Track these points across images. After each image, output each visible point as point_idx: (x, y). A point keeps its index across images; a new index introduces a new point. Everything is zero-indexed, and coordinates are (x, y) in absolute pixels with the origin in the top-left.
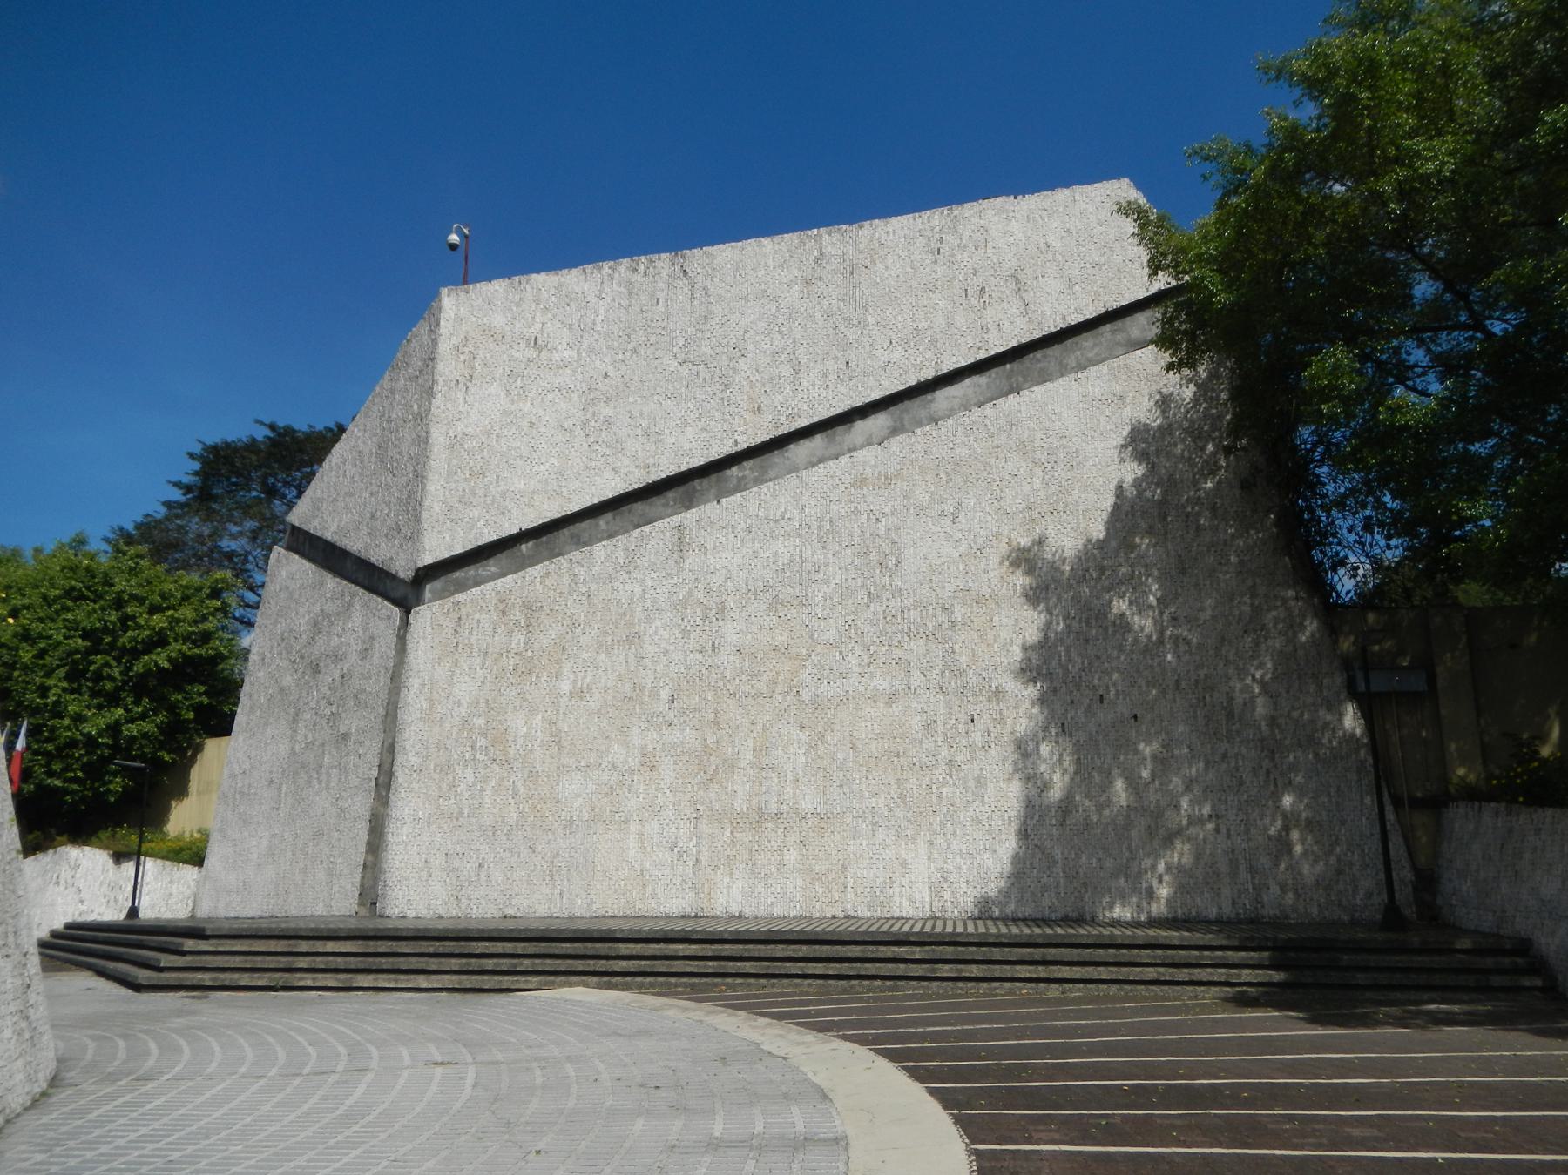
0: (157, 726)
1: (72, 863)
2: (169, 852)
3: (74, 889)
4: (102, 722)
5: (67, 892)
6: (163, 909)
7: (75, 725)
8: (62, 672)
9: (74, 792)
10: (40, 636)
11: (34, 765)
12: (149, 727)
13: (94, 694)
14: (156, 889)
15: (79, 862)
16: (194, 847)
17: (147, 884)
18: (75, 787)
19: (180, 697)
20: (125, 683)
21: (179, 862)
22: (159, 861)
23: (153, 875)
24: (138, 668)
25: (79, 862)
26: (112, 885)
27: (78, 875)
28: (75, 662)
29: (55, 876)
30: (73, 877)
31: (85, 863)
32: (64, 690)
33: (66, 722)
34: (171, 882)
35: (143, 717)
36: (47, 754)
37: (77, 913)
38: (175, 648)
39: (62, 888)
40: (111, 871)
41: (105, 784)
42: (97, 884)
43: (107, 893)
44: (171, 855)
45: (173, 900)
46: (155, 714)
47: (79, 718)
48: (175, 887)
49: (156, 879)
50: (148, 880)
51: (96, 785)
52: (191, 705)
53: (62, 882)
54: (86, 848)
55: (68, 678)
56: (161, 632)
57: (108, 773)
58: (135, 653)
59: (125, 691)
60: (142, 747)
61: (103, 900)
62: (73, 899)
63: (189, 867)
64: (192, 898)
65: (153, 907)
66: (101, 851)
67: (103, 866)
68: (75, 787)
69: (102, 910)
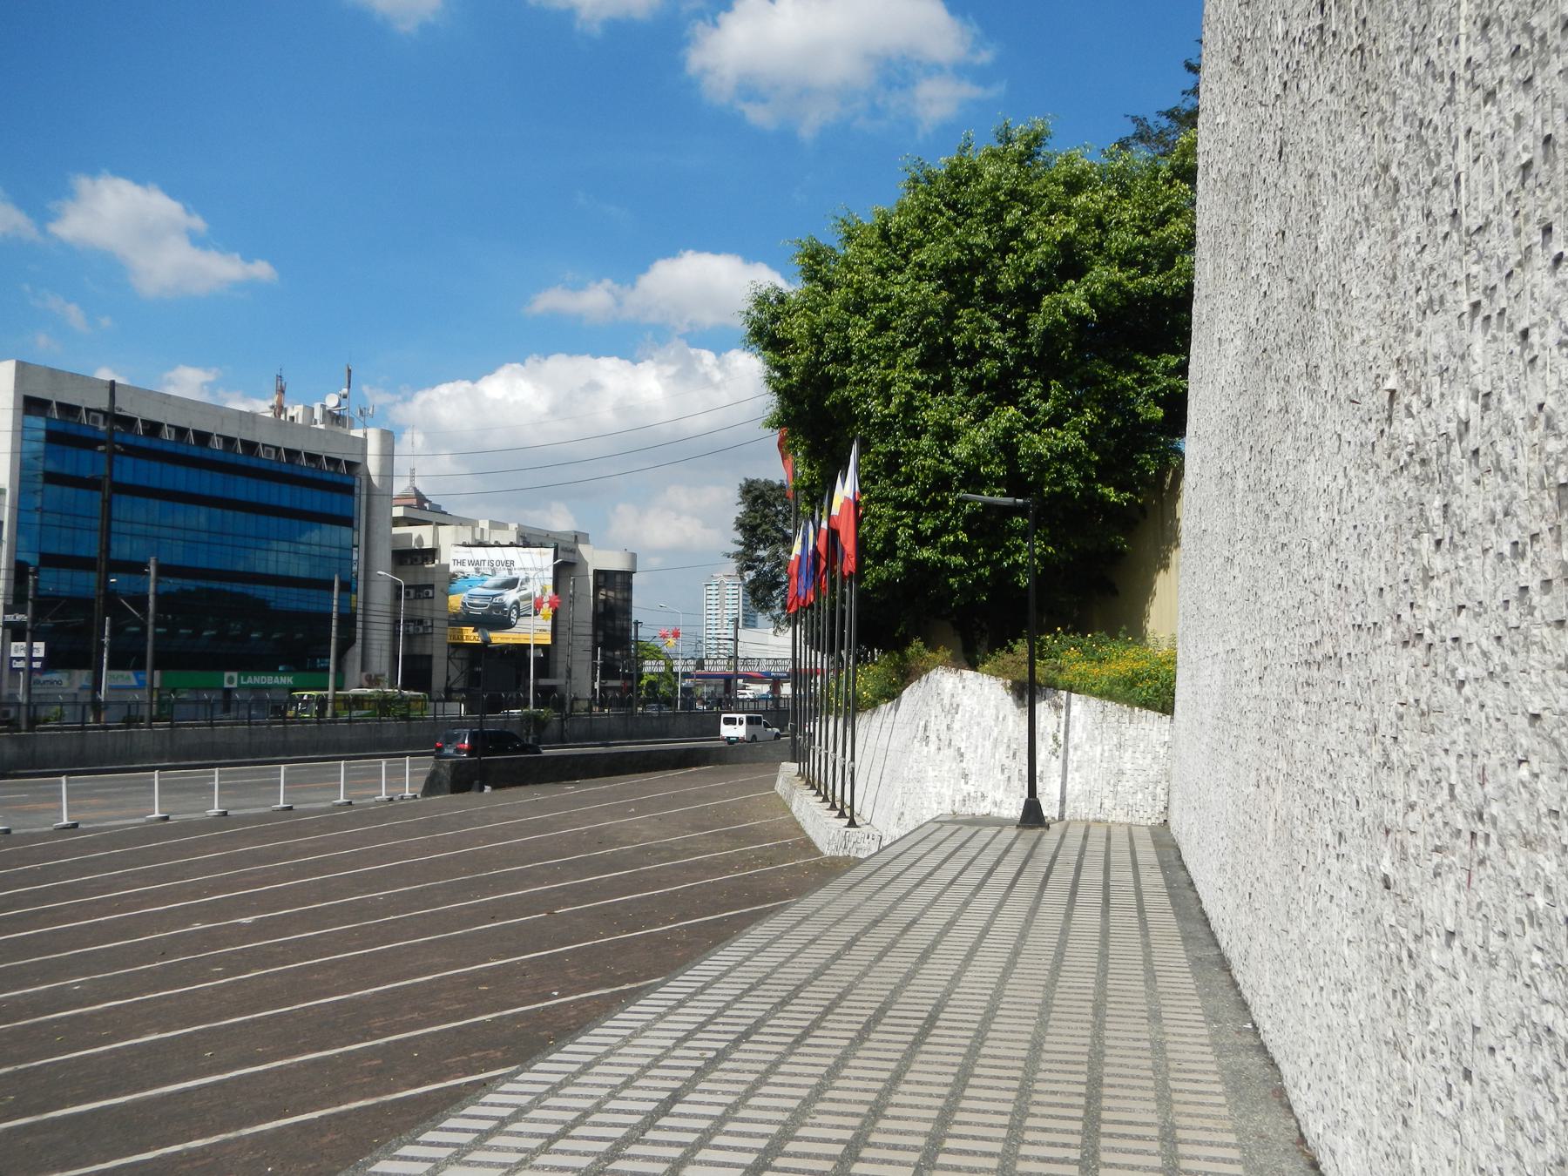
0: (1084, 437)
1: (946, 701)
2: (1112, 683)
3: (952, 752)
4: (980, 436)
5: (940, 757)
6: (1108, 804)
7: (941, 447)
8: (911, 355)
9: (957, 571)
10: (876, 298)
11: (898, 527)
12: (1070, 439)
13: (974, 386)
14: (1092, 760)
15: (957, 700)
16: (1163, 674)
17: (1076, 749)
18: (957, 560)
19: (1128, 380)
20: (1021, 360)
21: (1131, 705)
22: (1094, 701)
23: (1084, 728)
24: (1038, 323)
25: (957, 700)
26: (1014, 746)
27: (956, 726)
28: (929, 333)
29: (922, 723)
30: (948, 728)
31: (966, 701)
32: (918, 386)
33: (925, 442)
34: (1120, 746)
35: (1057, 420)
36: (909, 505)
37: (958, 798)
38: (1102, 274)
39: (933, 747)
40: (1010, 719)
41: (1008, 554)
42: (988, 745)
43: (1007, 762)
44: (1119, 689)
45: (1127, 784)
46: (1079, 411)
47: (947, 435)
48: (1128, 755)
49: (1091, 738)
50: (1077, 740)
51: (996, 555)
52: (1154, 395)
53: (933, 737)
54: (968, 674)
55: (923, 364)
56: (1067, 244)
57: (1012, 532)
58: (1028, 298)
59: (1023, 376)
60: (1061, 476)
61: (999, 776)
62: (950, 770)
63: (1152, 714)
64: (1164, 784)
65: (1090, 794)
66: (993, 679)
67: (997, 707)
68: (957, 560)
69: (999, 795)
